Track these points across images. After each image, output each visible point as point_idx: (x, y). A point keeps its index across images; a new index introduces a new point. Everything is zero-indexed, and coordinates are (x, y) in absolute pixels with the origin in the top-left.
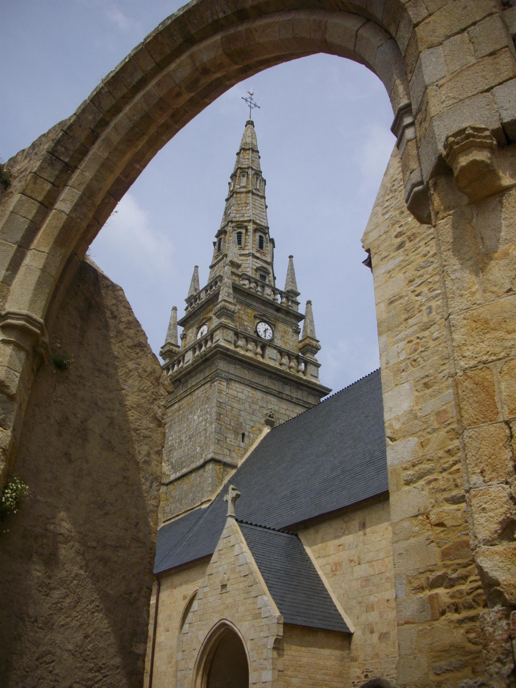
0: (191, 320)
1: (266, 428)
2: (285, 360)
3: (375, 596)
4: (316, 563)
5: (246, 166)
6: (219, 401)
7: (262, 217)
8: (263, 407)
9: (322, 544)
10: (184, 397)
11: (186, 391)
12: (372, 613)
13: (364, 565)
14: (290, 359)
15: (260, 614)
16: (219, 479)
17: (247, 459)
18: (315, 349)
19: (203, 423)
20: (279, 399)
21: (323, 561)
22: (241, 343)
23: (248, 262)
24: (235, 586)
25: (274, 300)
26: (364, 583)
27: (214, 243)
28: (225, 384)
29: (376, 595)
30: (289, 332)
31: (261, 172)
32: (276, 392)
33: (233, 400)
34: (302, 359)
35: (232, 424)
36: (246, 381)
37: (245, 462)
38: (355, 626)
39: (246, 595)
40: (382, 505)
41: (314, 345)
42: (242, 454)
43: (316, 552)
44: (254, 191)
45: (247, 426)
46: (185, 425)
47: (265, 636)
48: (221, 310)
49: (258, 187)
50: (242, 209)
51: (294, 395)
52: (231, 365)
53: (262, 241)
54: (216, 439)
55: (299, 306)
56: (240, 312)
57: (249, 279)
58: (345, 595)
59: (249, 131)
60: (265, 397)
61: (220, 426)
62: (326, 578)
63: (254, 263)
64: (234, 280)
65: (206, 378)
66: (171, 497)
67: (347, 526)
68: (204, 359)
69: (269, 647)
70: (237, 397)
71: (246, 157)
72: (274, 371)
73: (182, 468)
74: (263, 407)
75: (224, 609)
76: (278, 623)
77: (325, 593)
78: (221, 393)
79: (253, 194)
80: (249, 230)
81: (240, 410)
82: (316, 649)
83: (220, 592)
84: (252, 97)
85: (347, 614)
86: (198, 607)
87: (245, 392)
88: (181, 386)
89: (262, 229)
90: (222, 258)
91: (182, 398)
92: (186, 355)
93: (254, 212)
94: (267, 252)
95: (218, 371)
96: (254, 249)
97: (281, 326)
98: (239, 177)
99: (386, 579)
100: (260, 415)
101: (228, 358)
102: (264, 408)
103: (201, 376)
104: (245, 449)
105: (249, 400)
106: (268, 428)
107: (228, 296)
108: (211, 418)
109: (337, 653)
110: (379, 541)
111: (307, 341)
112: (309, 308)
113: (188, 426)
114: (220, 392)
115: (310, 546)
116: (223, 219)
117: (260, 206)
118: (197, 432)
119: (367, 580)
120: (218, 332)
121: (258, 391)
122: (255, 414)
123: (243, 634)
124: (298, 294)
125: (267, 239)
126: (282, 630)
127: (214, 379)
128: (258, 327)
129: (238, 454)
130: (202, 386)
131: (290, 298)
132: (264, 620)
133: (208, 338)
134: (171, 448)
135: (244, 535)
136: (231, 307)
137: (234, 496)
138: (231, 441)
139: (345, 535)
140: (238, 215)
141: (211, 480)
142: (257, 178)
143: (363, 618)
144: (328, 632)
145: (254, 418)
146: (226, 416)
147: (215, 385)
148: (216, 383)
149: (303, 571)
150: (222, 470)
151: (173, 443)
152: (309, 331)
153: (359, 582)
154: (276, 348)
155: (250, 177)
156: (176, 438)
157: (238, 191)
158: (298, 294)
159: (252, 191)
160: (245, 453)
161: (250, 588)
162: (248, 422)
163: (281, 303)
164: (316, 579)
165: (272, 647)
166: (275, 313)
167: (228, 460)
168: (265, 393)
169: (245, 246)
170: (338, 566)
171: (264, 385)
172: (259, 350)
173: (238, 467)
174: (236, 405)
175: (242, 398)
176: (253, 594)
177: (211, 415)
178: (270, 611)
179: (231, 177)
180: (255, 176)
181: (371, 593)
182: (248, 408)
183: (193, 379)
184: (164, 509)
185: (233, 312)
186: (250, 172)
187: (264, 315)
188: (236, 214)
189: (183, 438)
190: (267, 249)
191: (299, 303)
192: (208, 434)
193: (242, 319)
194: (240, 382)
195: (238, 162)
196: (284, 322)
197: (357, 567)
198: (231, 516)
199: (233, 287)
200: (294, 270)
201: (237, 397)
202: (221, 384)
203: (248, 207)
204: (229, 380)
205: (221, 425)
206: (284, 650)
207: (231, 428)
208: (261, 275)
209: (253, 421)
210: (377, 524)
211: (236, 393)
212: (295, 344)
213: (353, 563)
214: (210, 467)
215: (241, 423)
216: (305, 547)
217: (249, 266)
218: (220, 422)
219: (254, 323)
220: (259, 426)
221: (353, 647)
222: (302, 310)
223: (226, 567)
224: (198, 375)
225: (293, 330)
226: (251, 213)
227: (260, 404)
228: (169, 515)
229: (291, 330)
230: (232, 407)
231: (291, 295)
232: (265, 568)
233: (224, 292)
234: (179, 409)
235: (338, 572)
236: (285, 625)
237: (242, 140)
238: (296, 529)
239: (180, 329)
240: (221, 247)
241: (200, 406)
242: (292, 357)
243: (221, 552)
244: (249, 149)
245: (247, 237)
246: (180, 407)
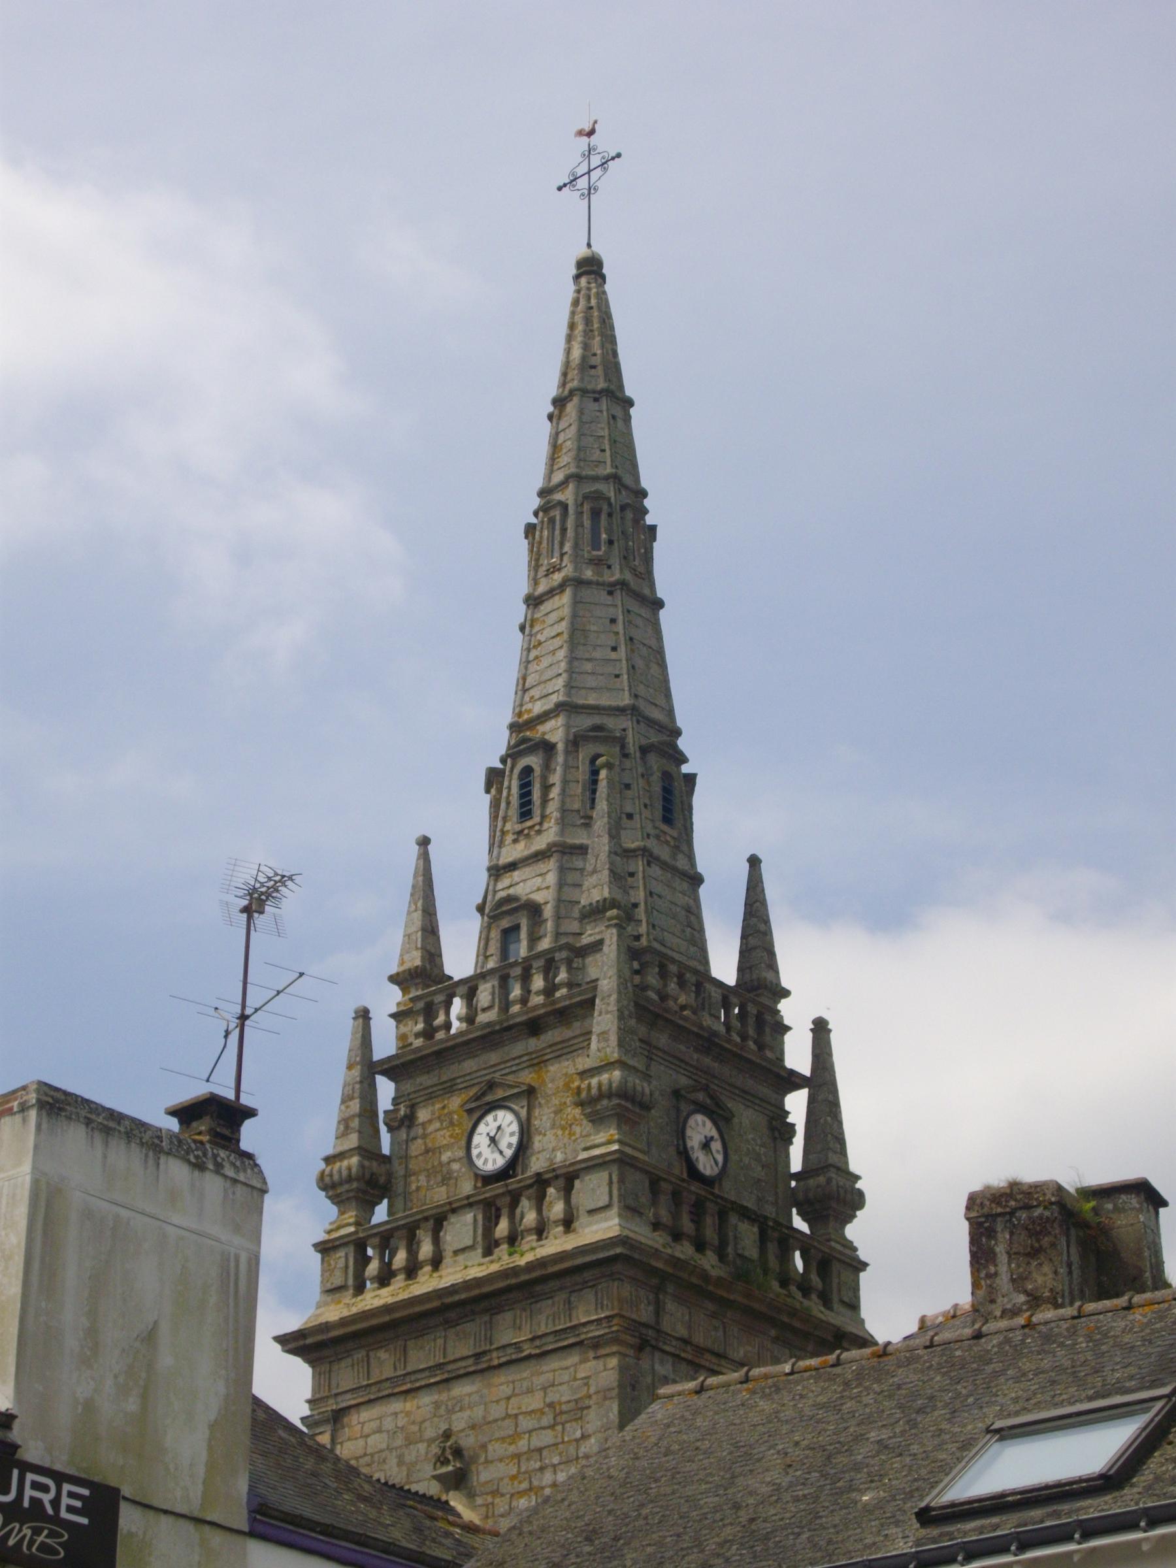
32: (471, 1361)
60: (444, 1396)
121: (422, 1393)
194: (370, 1401)
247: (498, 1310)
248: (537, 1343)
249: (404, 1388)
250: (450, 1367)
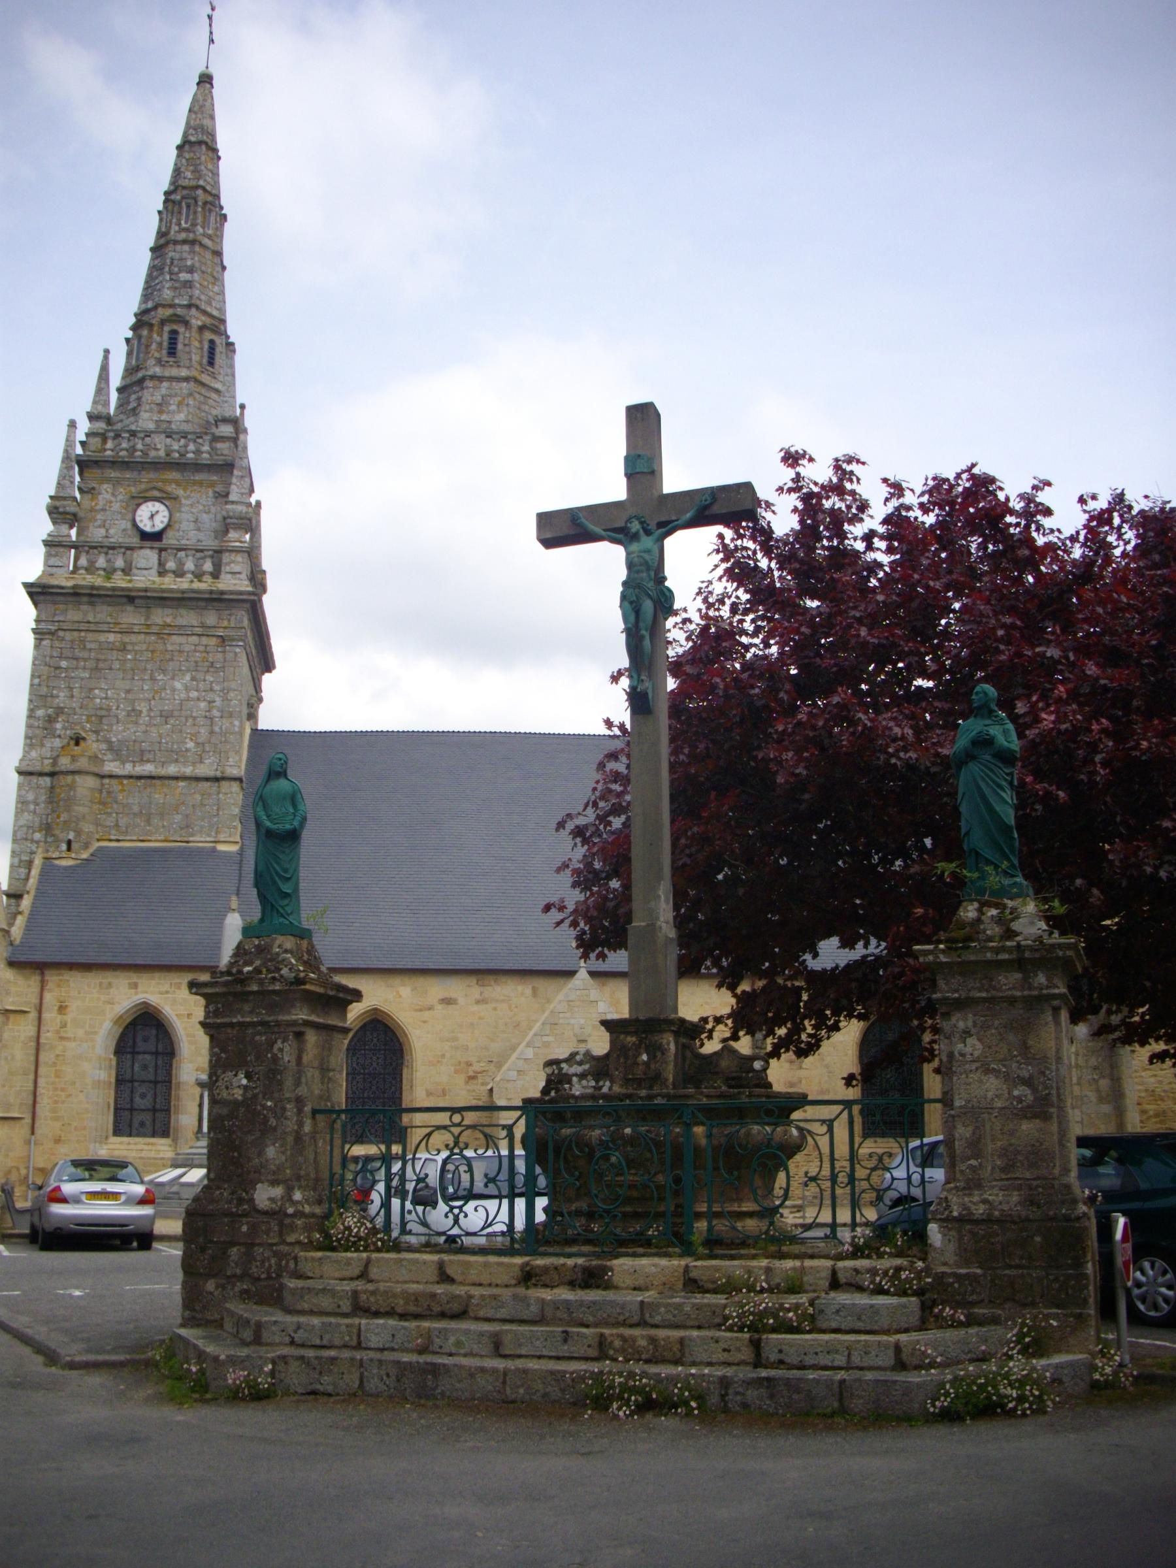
48: (242, 519)
66: (116, 802)
68: (214, 596)
73: (142, 760)
90: (187, 379)
127: (233, 640)
134: (104, 713)
183: (169, 611)
189: (143, 707)
224: (184, 612)
228: (113, 832)
234: (123, 649)
241: (188, 671)
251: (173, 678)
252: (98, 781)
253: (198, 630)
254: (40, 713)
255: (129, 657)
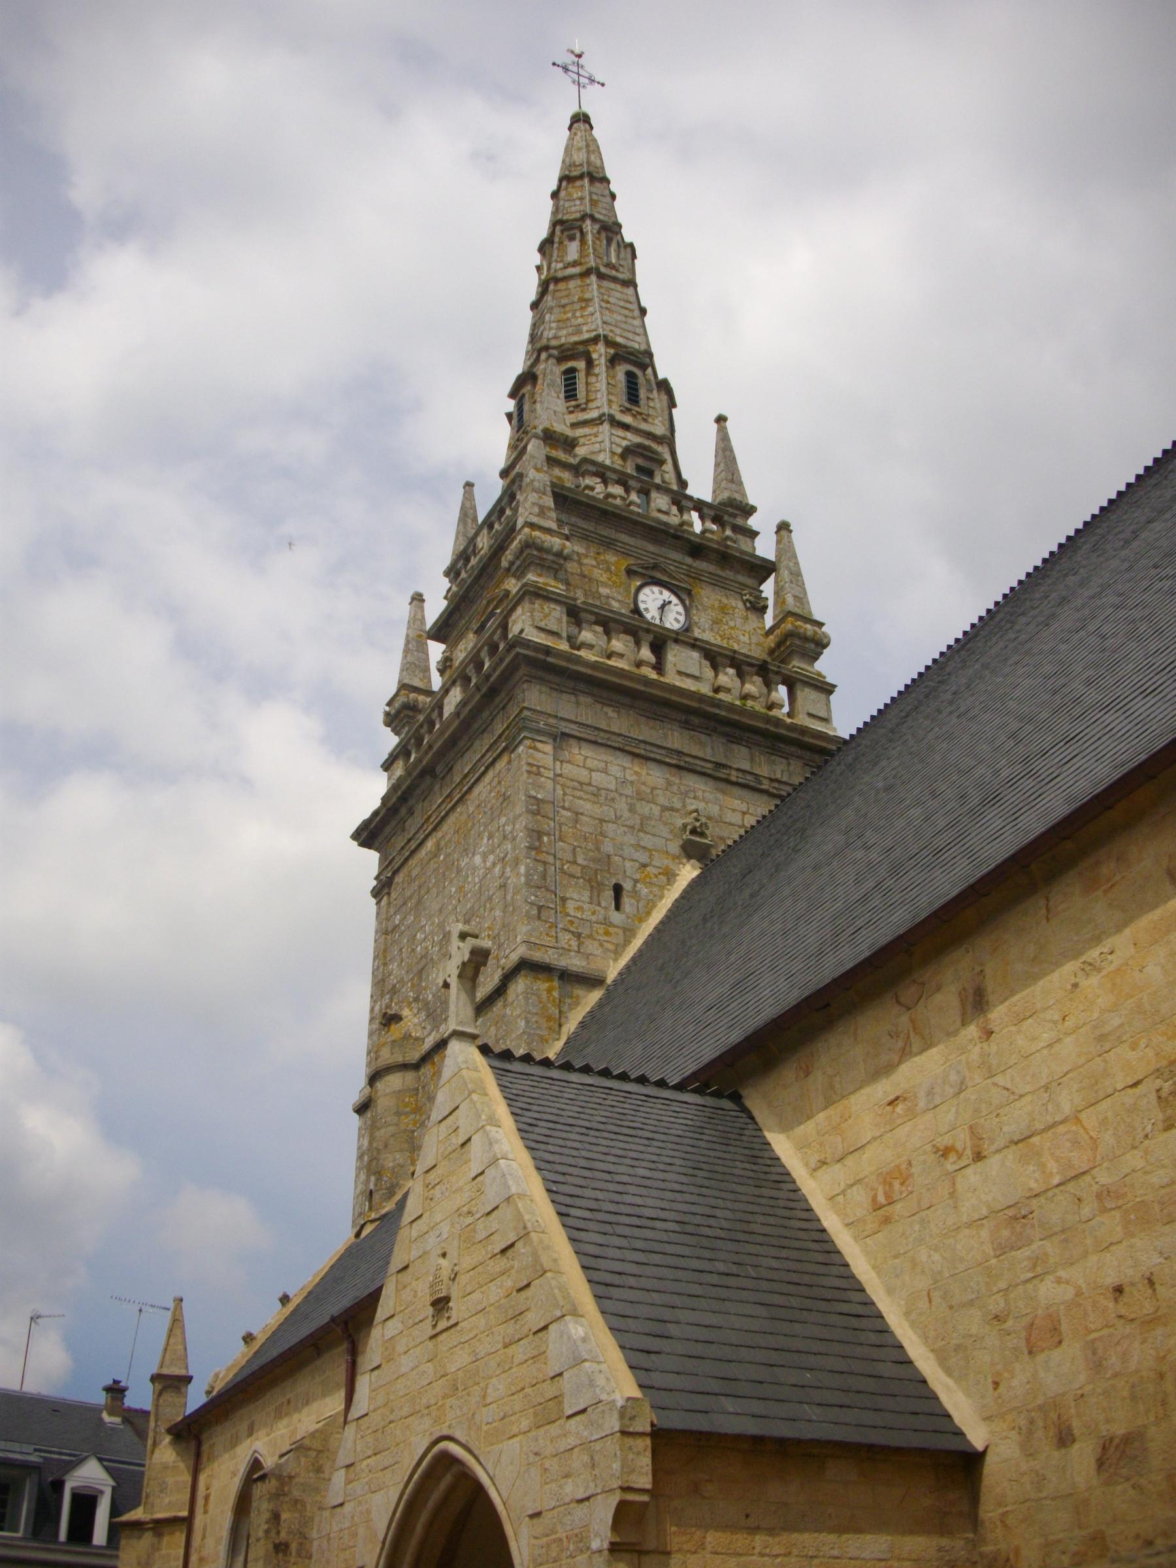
0: (461, 617)
1: (688, 867)
2: (728, 677)
3: (1059, 1281)
4: (815, 1189)
5: (578, 215)
6: (535, 798)
7: (631, 328)
8: (672, 809)
9: (830, 1111)
10: (447, 814)
11: (449, 795)
12: (1056, 1355)
13: (998, 1157)
14: (740, 675)
15: (558, 1398)
16: (549, 1019)
17: (634, 960)
18: (812, 646)
19: (497, 869)
20: (722, 785)
21: (837, 1175)
22: (586, 635)
23: (599, 439)
24: (477, 1296)
25: (683, 524)
26: (1005, 1233)
27: (509, 416)
28: (549, 748)
29: (1061, 1273)
30: (734, 609)
31: (620, 226)
32: (709, 765)
33: (578, 794)
34: (777, 673)
35: (580, 861)
36: (614, 737)
37: (628, 967)
38: (987, 1419)
39: (510, 1329)
40: (1042, 902)
41: (809, 633)
42: (617, 945)
43: (809, 1146)
44: (603, 270)
45: (628, 864)
46: (453, 890)
47: (580, 1496)
48: (522, 552)
49: (614, 261)
50: (574, 316)
51: (764, 770)
52: (565, 697)
53: (636, 384)
54: (532, 904)
55: (757, 540)
56: (586, 561)
57: (602, 473)
58: (936, 1295)
59: (578, 138)
61: (541, 869)
62: (856, 1238)
63: (618, 440)
64: (559, 478)
65: (495, 742)
67: (912, 1021)
68: (484, 690)
69: (595, 1544)
70: (590, 784)
71: (575, 196)
72: (694, 704)
74: (672, 809)
75: (445, 1397)
76: (624, 1433)
77: (855, 1296)
78: (539, 774)
79: (601, 276)
80: (596, 363)
81: (602, 821)
82: (824, 1537)
83: (431, 1332)
84: (581, 61)
85: (949, 1372)
86: (371, 1399)
87: (614, 769)
88: (437, 787)
89: (631, 354)
91: (443, 818)
92: (446, 701)
93: (605, 318)
94: (651, 412)
95: (526, 713)
96: (615, 407)
97: (708, 596)
98: (561, 243)
99: (1099, 1196)
100: (664, 831)
101: (551, 677)
102: (677, 811)
103: (481, 746)
104: (625, 930)
105: (628, 791)
106: (693, 867)
107: (542, 512)
108: (514, 849)
109: (919, 1544)
110: (1050, 1046)
111: (788, 626)
112: (785, 540)
113: (460, 889)
114: (535, 771)
115: (786, 1127)
116: (527, 352)
117: (622, 303)
118: (483, 898)
119: (1017, 1218)
120: (519, 610)
121: (651, 765)
122: (649, 829)
123: (505, 1494)
124: (750, 510)
125: (648, 381)
126: (646, 1461)
127: (514, 739)
128: (641, 597)
129: (607, 945)
130: (487, 769)
131: (726, 518)
132: (573, 1421)
133: (496, 638)
134: (424, 961)
135: (510, 1100)
136: (556, 542)
137: (467, 957)
138: (578, 909)
139: (912, 1055)
140: (565, 332)
141: (523, 1023)
142: (609, 241)
143: (1018, 1382)
144: (868, 1455)
145: (647, 841)
146: (561, 839)
147: (519, 756)
148: (521, 748)
149: (760, 1219)
150: (556, 994)
151: (426, 948)
152: (790, 599)
153: (985, 1234)
154: (695, 645)
155: (590, 237)
156: (432, 933)
157: (560, 274)
158: (750, 510)
159: (597, 269)
160: (627, 942)
161: (524, 1294)
162: (628, 851)
163: (704, 532)
164: (816, 1246)
165: (606, 1545)
166: (689, 560)
167: (575, 963)
168: (674, 770)
169: (588, 401)
170: (896, 1185)
171: (669, 746)
172: (646, 653)
173: (609, 981)
174: (587, 807)
175: (606, 786)
176: (534, 1320)
177: (514, 839)
178: (592, 1383)
179: (541, 249)
180: (603, 235)
181: (1039, 1269)
182: (626, 814)
184: (412, 1138)
185: (559, 554)
186: (588, 226)
187: (655, 567)
188: (559, 328)
190: (651, 404)
191: (756, 534)
192: (509, 897)
193: (590, 579)
194: (595, 743)
195: (555, 211)
196: (718, 583)
197: (969, 1171)
198: (457, 1034)
199: (556, 496)
200: (732, 451)
201: (590, 784)
202: (535, 748)
203: (591, 309)
204: (561, 739)
205: (545, 863)
206: (669, 1553)
207: (576, 870)
208: (639, 468)
209: (644, 848)
210: (1034, 978)
211: (585, 772)
212: (754, 639)
213: (952, 1157)
214: (520, 986)
215: (609, 856)
216: (770, 1136)
217: (603, 445)
218: (542, 857)
219: (628, 591)
220: (667, 862)
221: (989, 1511)
222: (765, 547)
223: (445, 1228)
224: (477, 743)
225: (744, 602)
226: (599, 322)
227: (661, 800)
229: (740, 605)
230: (577, 814)
231: (732, 511)
232: (587, 1214)
233: (528, 505)
235: (898, 1207)
236: (660, 1437)
237: (563, 161)
238: (734, 1075)
239: (436, 650)
240: (526, 416)
241: (486, 826)
242: (746, 668)
243: (432, 1176)
244: (581, 177)
245: (592, 379)
246: (438, 844)
247: (738, 741)
248: (776, 785)
249: (637, 751)
250: (688, 759)
251: (474, 854)
252: (410, 1076)
253: (489, 758)
254: (377, 1008)
255: (442, 857)
